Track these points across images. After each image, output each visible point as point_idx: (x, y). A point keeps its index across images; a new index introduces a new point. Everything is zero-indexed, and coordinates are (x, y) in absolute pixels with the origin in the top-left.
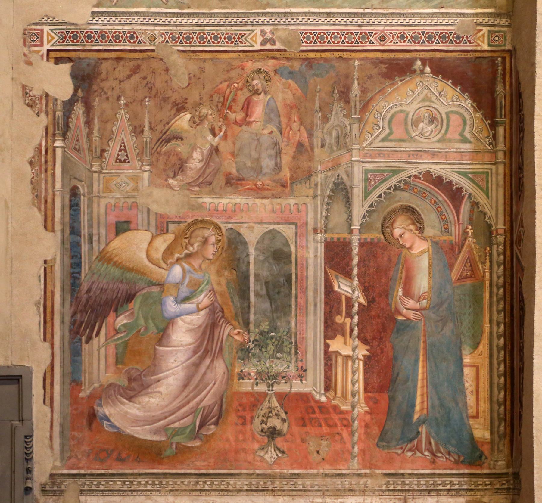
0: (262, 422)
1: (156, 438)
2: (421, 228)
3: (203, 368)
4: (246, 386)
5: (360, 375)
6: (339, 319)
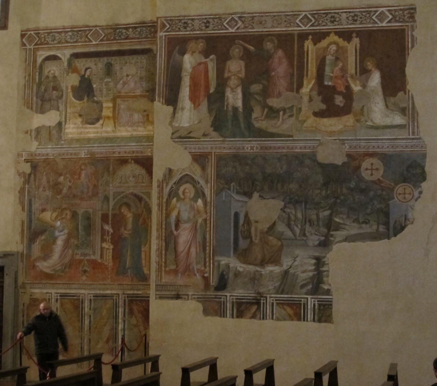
0: (82, 268)
1: (52, 273)
2: (130, 210)
3: (65, 252)
4: (78, 257)
5: (111, 254)
6: (105, 237)
